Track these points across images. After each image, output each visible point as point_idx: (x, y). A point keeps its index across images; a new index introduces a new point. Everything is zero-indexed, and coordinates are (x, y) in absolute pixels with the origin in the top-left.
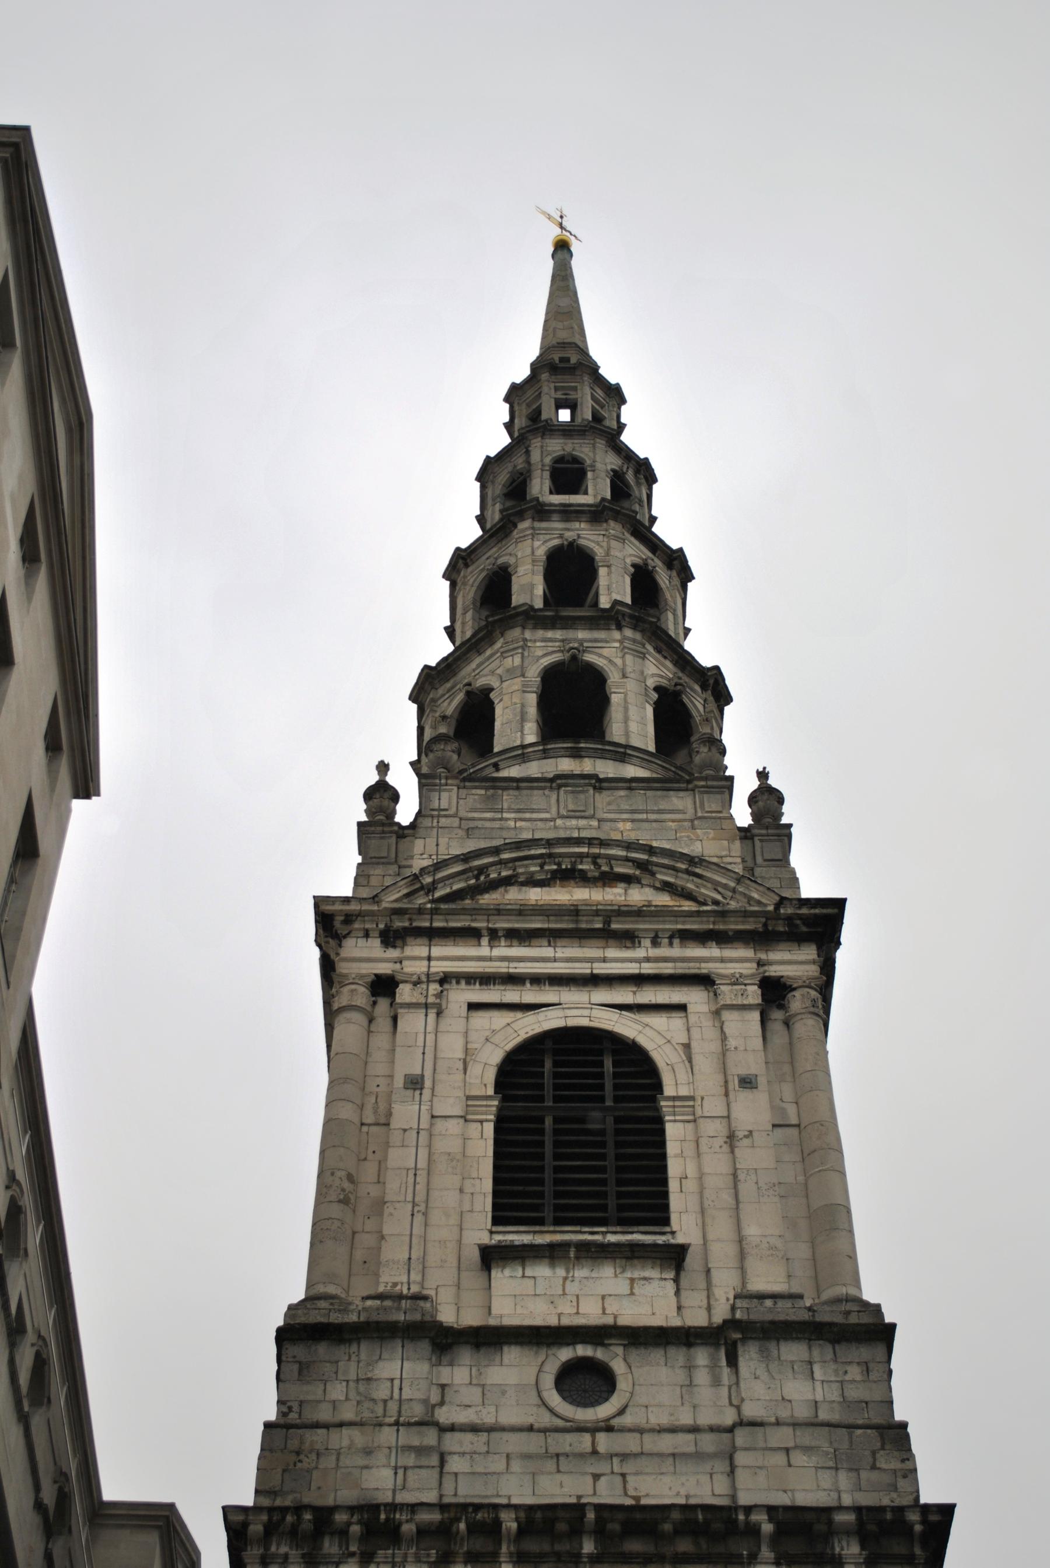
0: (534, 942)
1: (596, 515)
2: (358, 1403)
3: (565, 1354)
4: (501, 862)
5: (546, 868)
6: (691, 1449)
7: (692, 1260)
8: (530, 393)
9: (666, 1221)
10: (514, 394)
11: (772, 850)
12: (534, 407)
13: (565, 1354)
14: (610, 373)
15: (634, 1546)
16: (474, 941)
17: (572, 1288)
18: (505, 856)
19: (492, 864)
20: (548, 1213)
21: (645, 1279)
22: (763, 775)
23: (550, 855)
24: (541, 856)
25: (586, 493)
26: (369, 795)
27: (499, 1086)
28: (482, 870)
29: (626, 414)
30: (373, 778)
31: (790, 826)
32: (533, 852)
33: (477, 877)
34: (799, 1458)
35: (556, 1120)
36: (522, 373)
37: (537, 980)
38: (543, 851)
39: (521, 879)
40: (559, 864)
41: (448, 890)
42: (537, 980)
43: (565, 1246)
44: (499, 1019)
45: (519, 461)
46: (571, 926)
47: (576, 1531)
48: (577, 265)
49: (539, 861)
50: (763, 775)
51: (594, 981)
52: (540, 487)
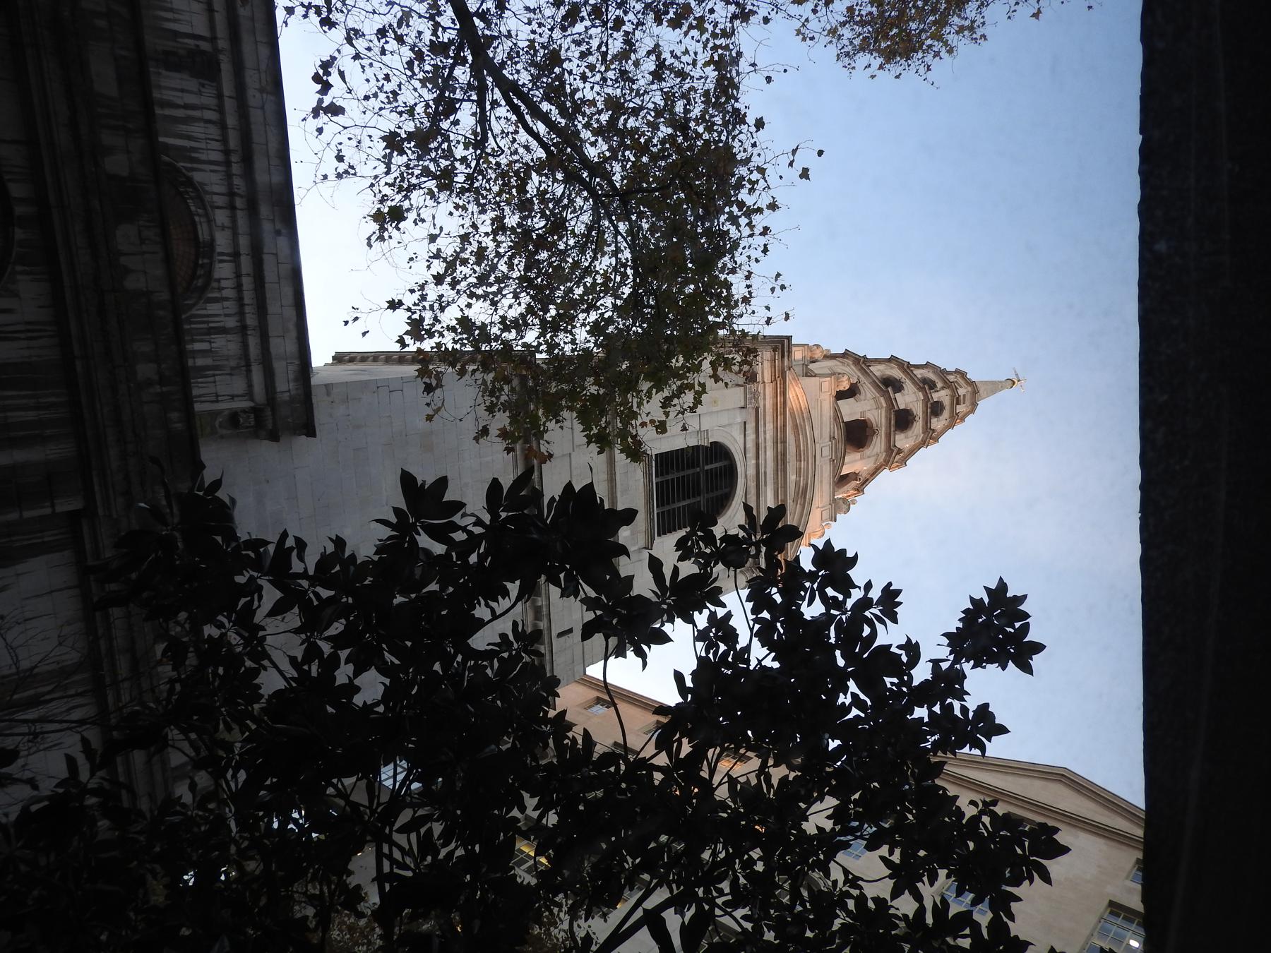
8: (961, 382)
9: (659, 535)
10: (962, 374)
48: (1006, 393)
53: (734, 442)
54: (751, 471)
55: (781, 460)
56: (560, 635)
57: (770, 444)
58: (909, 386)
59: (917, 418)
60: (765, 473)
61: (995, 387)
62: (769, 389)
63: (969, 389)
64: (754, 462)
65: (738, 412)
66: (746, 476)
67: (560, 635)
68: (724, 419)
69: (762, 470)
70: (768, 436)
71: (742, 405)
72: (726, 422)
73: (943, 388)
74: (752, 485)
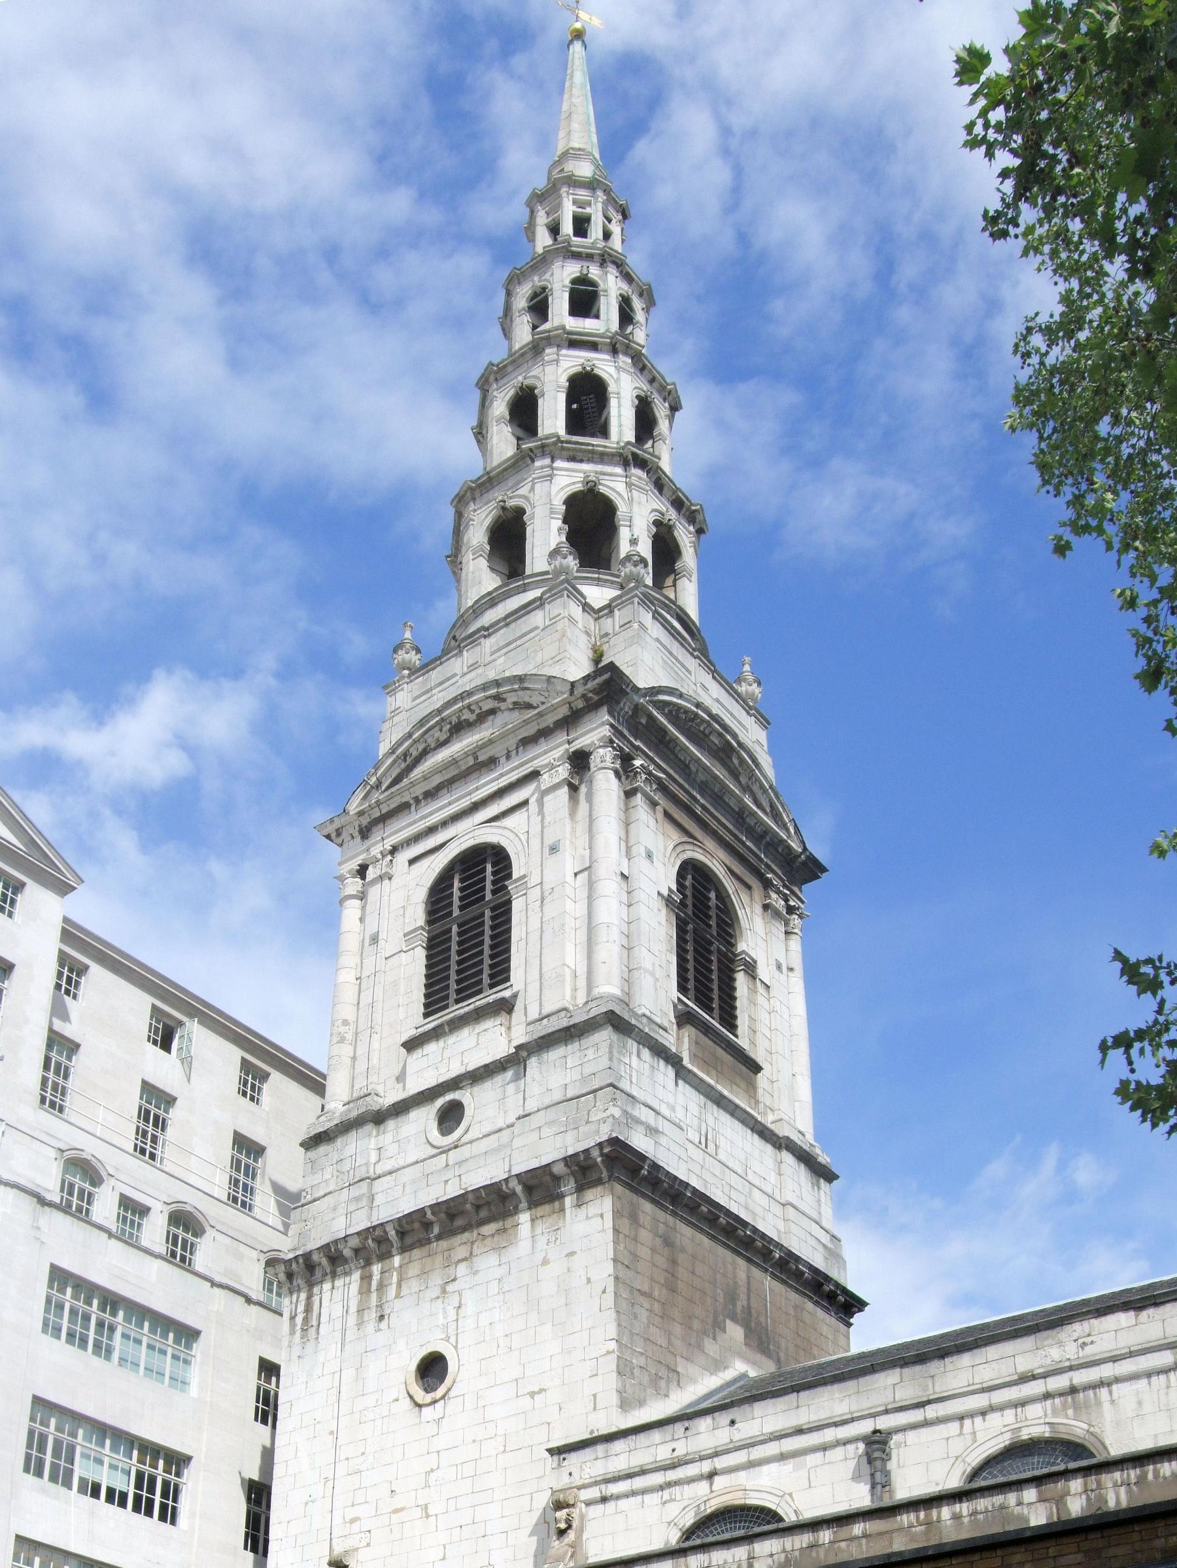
0: (440, 794)
2: (337, 1177)
3: (440, 1102)
4: (415, 742)
5: (444, 729)
6: (495, 1145)
13: (440, 1102)
15: (459, 1222)
16: (407, 811)
17: (447, 1053)
18: (415, 736)
19: (411, 746)
21: (485, 1030)
23: (443, 720)
24: (437, 723)
25: (597, 317)
28: (405, 755)
32: (432, 723)
33: (405, 760)
34: (546, 1132)
35: (459, 926)
37: (444, 824)
38: (437, 719)
39: (433, 745)
40: (451, 723)
41: (390, 780)
42: (444, 824)
43: (440, 1026)
44: (425, 863)
46: (456, 772)
47: (427, 1226)
49: (437, 728)
51: (476, 807)
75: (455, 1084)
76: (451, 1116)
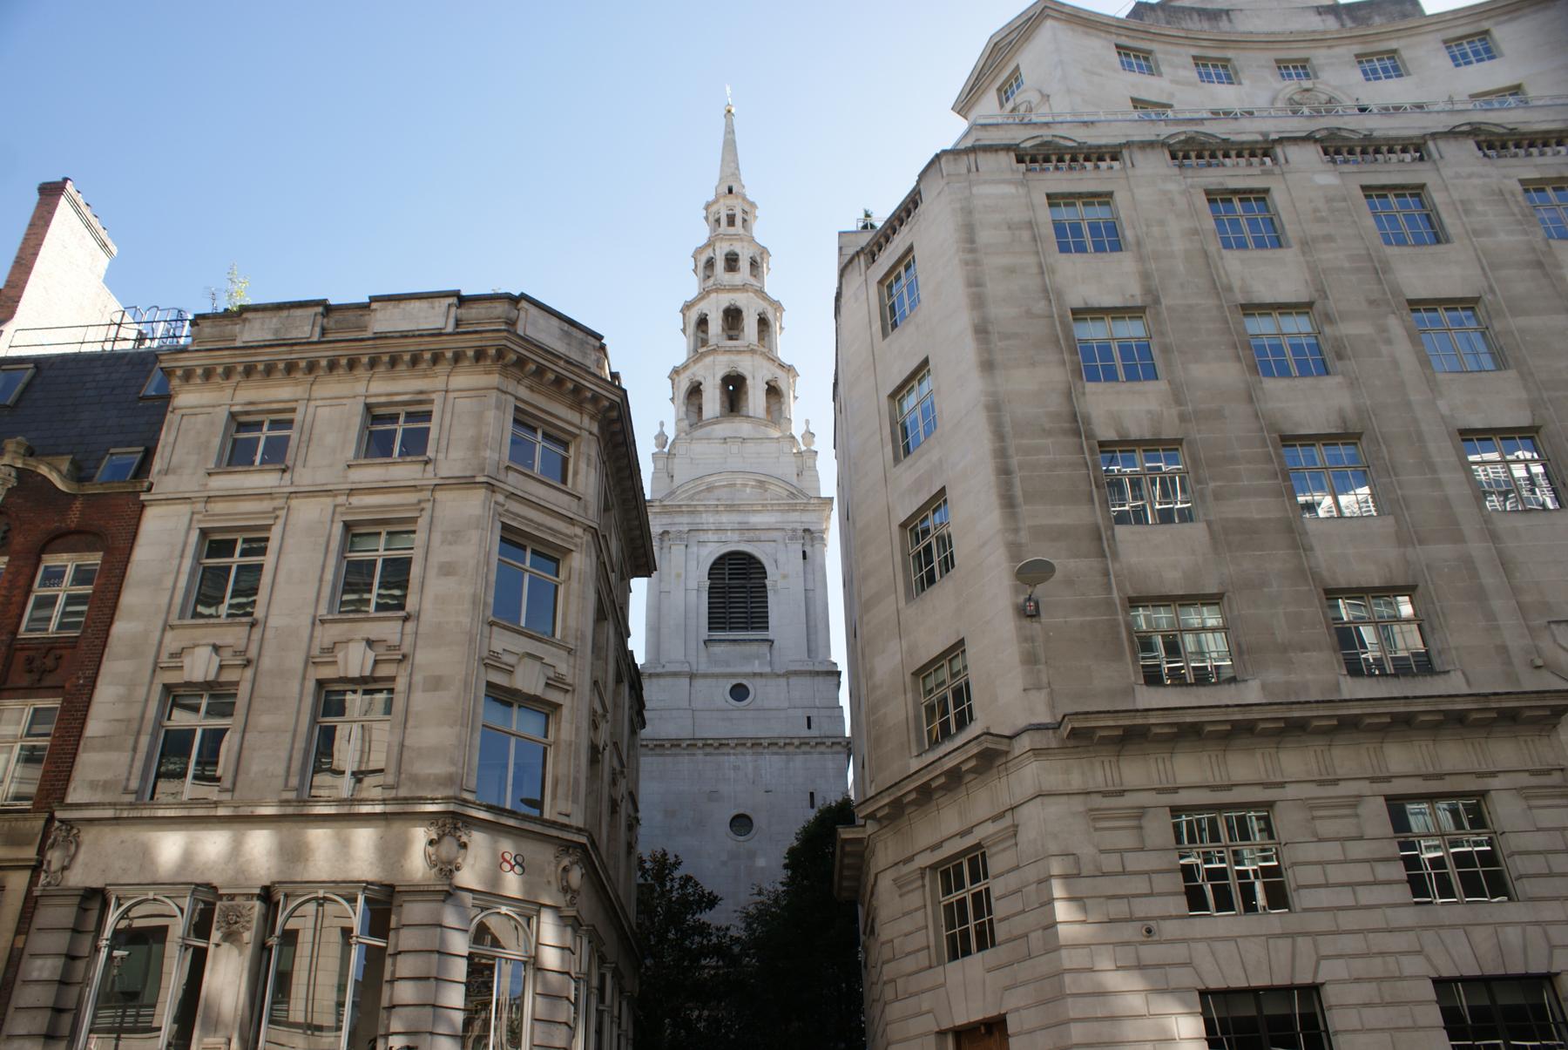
1: (744, 288)
7: (775, 643)
8: (714, 208)
10: (708, 206)
11: (809, 462)
12: (717, 216)
14: (750, 197)
20: (728, 626)
22: (807, 422)
26: (656, 438)
27: (709, 574)
29: (757, 213)
30: (657, 431)
31: (816, 452)
36: (711, 197)
45: (708, 253)
48: (736, 121)
50: (807, 422)
52: (720, 264)
53: (712, 552)
54: (736, 536)
55: (731, 508)
56: (809, 727)
57: (717, 518)
58: (703, 307)
59: (733, 302)
60: (739, 523)
61: (730, 146)
62: (678, 519)
63: (722, 201)
64: (729, 533)
65: (690, 550)
66: (739, 542)
67: (809, 727)
68: (692, 564)
69: (736, 526)
70: (711, 520)
71: (683, 547)
72: (695, 563)
73: (714, 250)
74: (751, 534)
75: (746, 675)
76: (739, 692)
